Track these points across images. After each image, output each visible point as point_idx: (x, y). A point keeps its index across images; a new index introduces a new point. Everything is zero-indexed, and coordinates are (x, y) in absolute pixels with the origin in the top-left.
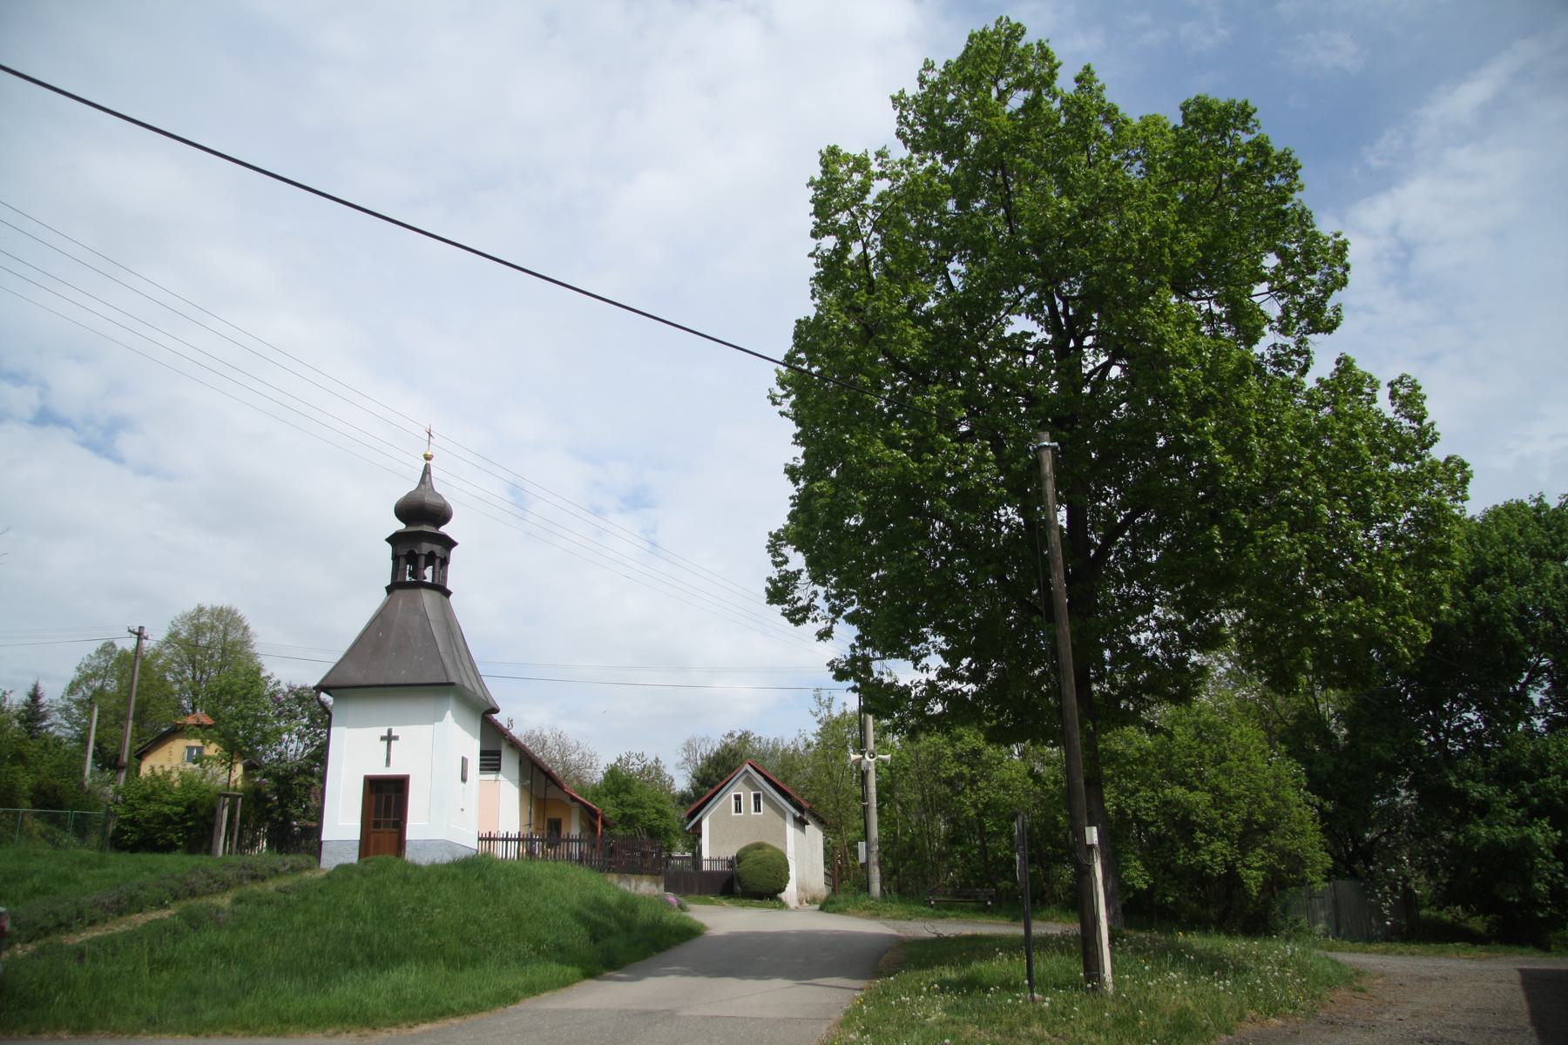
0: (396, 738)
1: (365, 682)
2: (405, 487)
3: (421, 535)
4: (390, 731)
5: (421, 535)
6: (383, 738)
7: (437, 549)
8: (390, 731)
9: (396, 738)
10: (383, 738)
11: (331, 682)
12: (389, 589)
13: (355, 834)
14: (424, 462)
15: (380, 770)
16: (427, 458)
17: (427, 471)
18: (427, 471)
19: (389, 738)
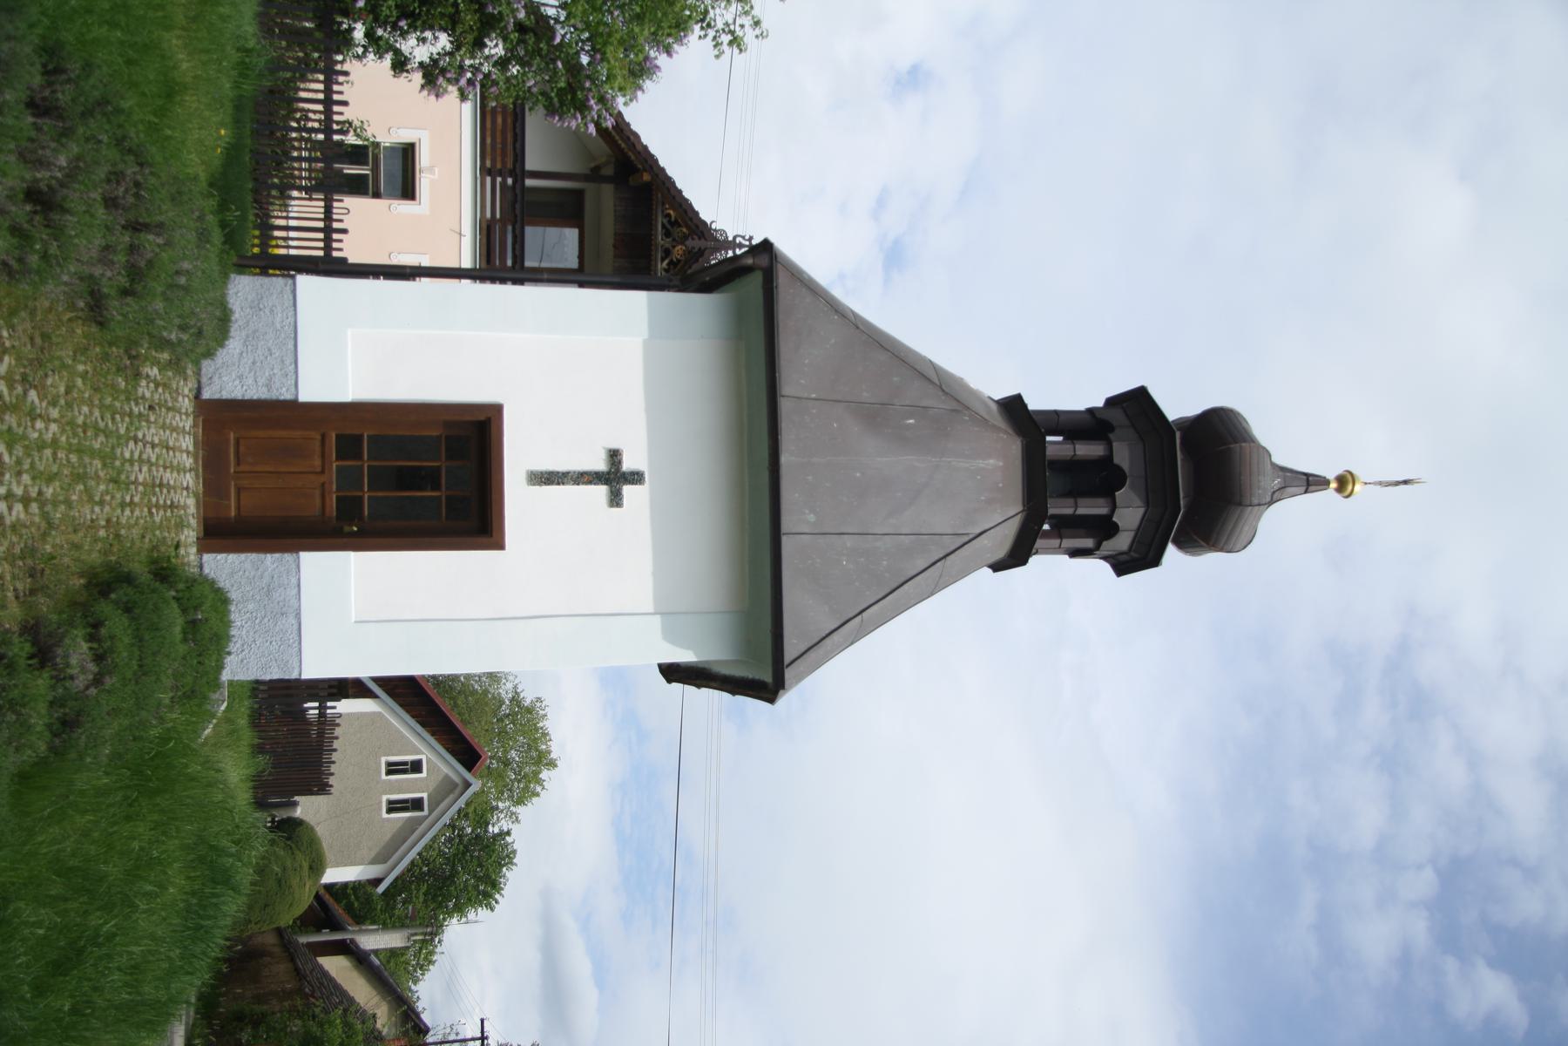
0: (615, 500)
1: (785, 406)
2: (1281, 436)
3: (1146, 481)
4: (636, 478)
5: (1146, 481)
6: (614, 456)
7: (1122, 542)
8: (636, 478)
9: (615, 500)
10: (614, 456)
11: (782, 279)
12: (1013, 407)
13: (313, 389)
14: (1331, 475)
15: (518, 455)
16: (1344, 483)
17: (1312, 483)
18: (1312, 483)
19: (614, 477)
